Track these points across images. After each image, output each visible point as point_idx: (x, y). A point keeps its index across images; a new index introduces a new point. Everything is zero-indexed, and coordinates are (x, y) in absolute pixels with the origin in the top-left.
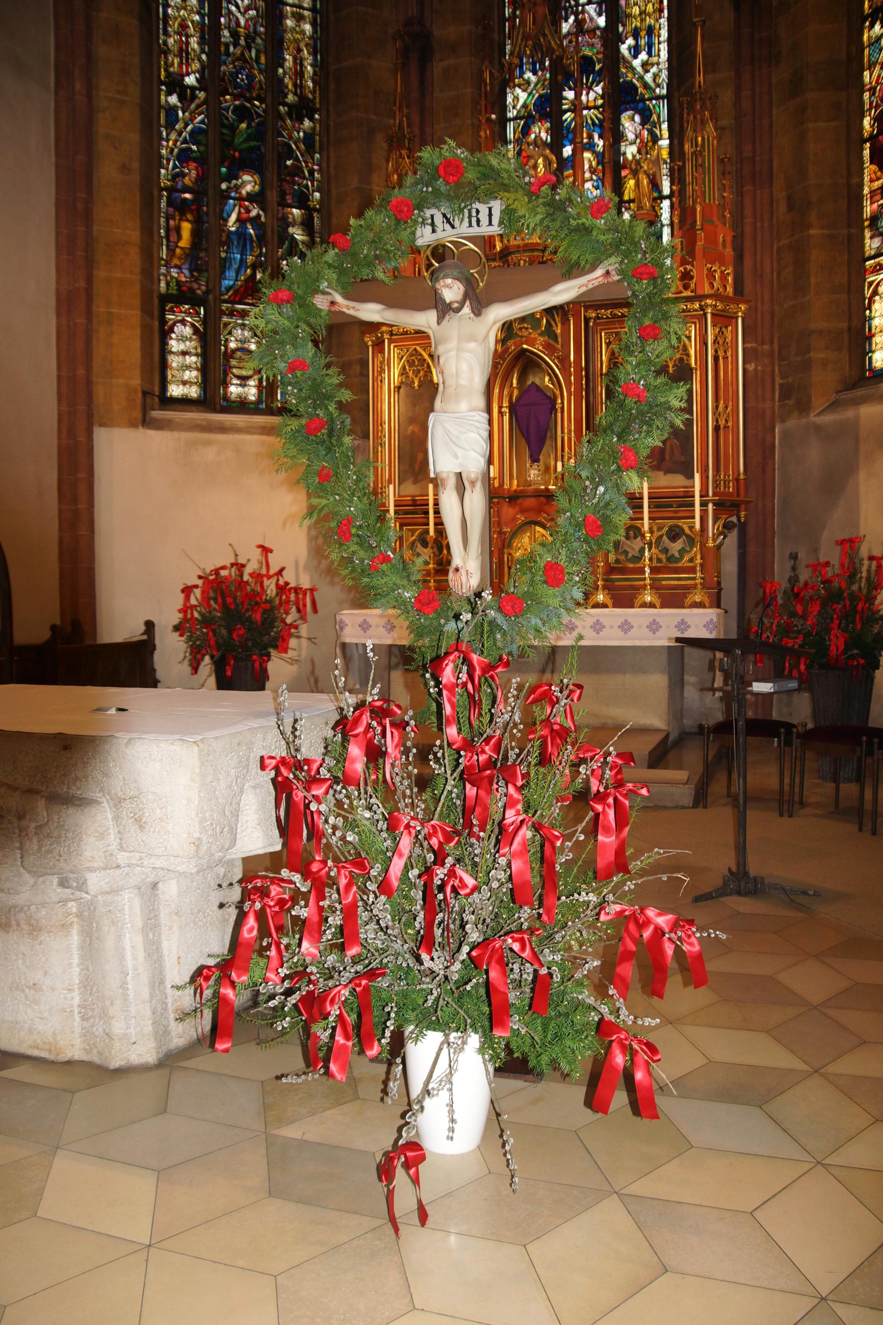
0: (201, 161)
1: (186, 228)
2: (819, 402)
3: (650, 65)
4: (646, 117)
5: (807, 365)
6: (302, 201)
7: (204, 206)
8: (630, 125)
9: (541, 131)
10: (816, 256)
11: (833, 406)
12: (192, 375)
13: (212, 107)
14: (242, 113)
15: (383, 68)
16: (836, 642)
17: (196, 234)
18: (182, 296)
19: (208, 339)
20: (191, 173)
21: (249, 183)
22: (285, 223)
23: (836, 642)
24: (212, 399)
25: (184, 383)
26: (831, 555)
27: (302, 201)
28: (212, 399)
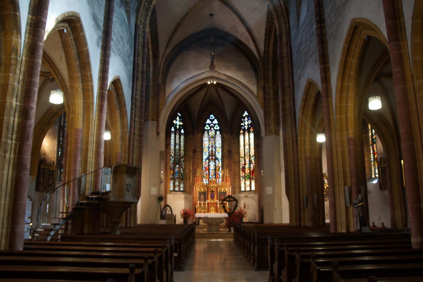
0: (174, 164)
1: (172, 171)
2: (237, 193)
3: (219, 155)
4: (219, 161)
5: (235, 190)
6: (182, 168)
7: (174, 169)
8: (217, 161)
9: (207, 161)
10: (237, 179)
11: (238, 194)
12: (172, 188)
13: (175, 158)
14: (177, 158)
15: (191, 154)
16: (240, 216)
17: (173, 172)
18: (172, 179)
19: (174, 183)
20: (173, 165)
21: (177, 166)
22: (181, 170)
23: (240, 216)
24: (174, 190)
25: (172, 189)
26: (239, 209)
27: (182, 168)
28: (174, 190)
